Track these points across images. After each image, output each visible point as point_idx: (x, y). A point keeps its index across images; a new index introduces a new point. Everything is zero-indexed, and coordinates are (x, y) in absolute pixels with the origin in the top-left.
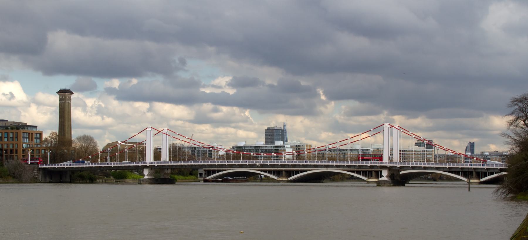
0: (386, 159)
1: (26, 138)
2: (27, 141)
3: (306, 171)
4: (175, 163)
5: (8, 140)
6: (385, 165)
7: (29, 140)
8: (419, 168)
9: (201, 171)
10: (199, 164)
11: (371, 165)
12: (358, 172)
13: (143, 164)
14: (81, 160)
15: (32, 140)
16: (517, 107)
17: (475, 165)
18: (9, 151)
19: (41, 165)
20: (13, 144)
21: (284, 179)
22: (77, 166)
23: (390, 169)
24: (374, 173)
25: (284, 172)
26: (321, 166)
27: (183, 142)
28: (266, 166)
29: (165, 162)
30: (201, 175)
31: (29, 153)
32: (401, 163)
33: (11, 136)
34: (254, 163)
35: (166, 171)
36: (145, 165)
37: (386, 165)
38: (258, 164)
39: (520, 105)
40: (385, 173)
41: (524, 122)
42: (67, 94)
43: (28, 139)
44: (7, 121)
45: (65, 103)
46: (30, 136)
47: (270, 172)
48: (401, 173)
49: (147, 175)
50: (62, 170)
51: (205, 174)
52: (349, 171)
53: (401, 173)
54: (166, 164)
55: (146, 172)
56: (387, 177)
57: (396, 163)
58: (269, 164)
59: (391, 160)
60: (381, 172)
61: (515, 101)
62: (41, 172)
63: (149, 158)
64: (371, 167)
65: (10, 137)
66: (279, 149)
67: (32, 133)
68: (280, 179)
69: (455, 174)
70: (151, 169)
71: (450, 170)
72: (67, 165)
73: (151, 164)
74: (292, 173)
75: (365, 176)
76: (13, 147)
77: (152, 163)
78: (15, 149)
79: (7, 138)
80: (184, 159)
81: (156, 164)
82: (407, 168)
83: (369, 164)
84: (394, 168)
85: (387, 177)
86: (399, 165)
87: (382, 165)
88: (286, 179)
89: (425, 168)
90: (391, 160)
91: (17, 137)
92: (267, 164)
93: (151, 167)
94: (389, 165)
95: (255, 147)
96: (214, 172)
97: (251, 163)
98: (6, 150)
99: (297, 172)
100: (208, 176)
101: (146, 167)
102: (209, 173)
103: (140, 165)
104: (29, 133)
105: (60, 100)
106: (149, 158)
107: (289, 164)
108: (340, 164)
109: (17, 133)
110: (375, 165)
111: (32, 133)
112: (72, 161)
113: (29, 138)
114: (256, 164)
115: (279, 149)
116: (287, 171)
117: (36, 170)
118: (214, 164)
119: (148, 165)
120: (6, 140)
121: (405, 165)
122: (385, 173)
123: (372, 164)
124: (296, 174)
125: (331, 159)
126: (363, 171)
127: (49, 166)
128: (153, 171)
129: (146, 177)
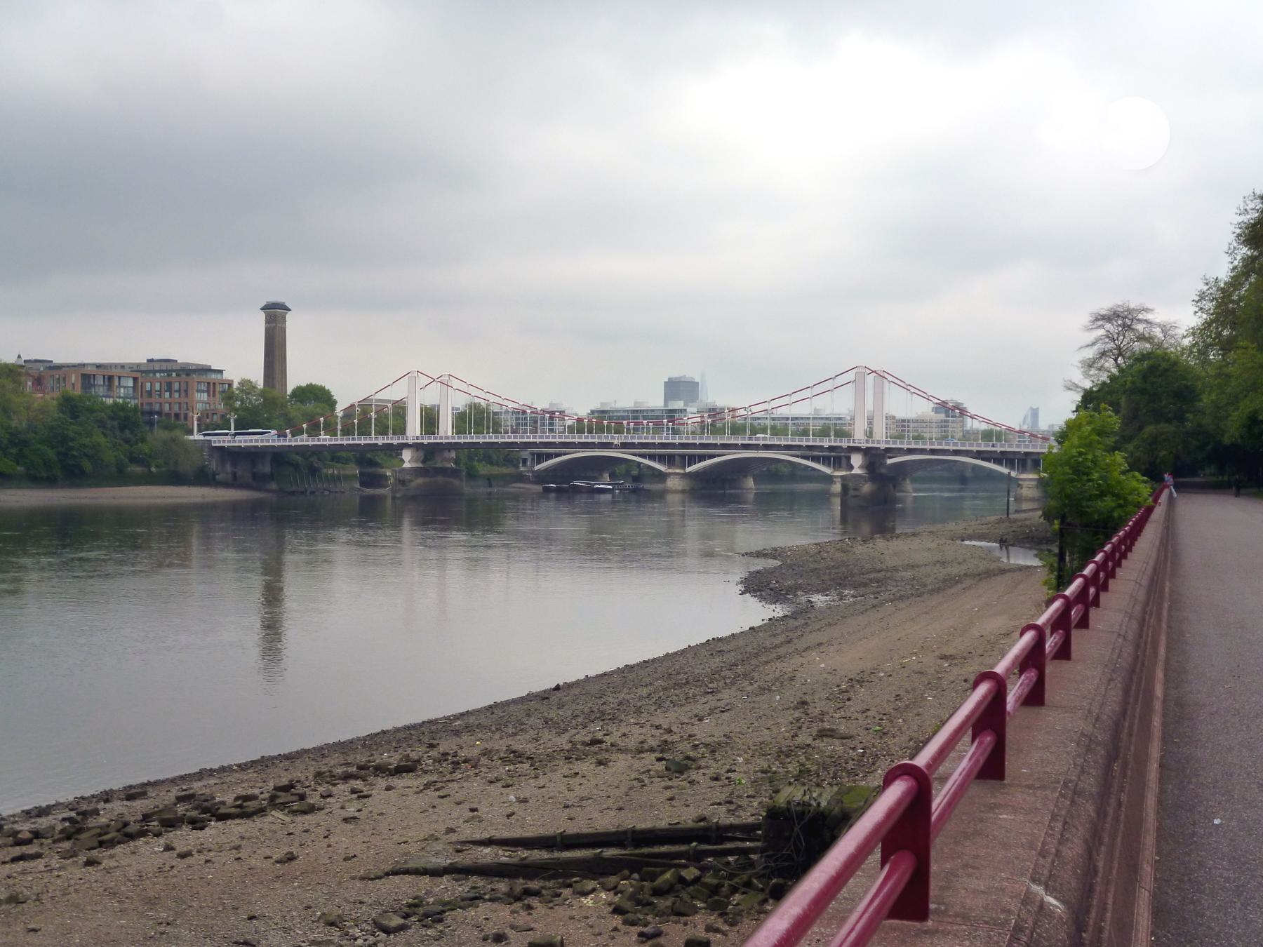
1: (204, 391)
2: (204, 396)
3: (719, 456)
4: (460, 438)
5: (171, 396)
7: (209, 395)
8: (922, 451)
9: (525, 454)
10: (506, 440)
11: (830, 444)
12: (816, 459)
13: (401, 441)
15: (214, 395)
16: (1101, 332)
17: (1027, 446)
18: (173, 415)
20: (180, 403)
21: (678, 471)
22: (280, 444)
23: (867, 452)
25: (677, 458)
26: (746, 447)
27: (477, 400)
28: (632, 446)
30: (525, 461)
31: (195, 419)
32: (887, 442)
34: (609, 441)
35: (446, 455)
36: (405, 441)
37: (859, 445)
38: (616, 442)
39: (1108, 326)
40: (857, 460)
41: (1116, 360)
43: (206, 394)
44: (176, 361)
45: (274, 327)
46: (211, 388)
47: (652, 457)
48: (889, 461)
50: (253, 450)
51: (533, 459)
52: (797, 456)
53: (889, 461)
55: (407, 455)
57: (878, 442)
58: (636, 441)
59: (869, 434)
60: (849, 458)
61: (1097, 320)
63: (414, 428)
64: (831, 448)
65: (176, 391)
66: (676, 415)
67: (214, 384)
68: (670, 471)
69: (994, 463)
70: (417, 450)
73: (416, 441)
74: (692, 459)
75: (829, 465)
76: (180, 409)
77: (418, 438)
78: (182, 413)
80: (496, 432)
81: (426, 441)
82: (900, 451)
83: (826, 444)
84: (874, 452)
85: (861, 467)
86: (883, 446)
87: (852, 445)
88: (682, 471)
89: (933, 452)
90: (869, 434)
91: (186, 391)
92: (633, 441)
93: (417, 447)
94: (864, 446)
95: (633, 411)
96: (549, 456)
97: (583, 440)
98: (168, 415)
99: (702, 458)
100: (539, 463)
101: (406, 446)
102: (540, 458)
103: (395, 441)
104: (209, 383)
105: (267, 322)
106: (414, 428)
107: (674, 441)
108: (709, 442)
109: (187, 382)
110: (838, 444)
111: (214, 384)
113: (208, 392)
114: (613, 441)
115: (676, 415)
116: (683, 456)
117: (206, 450)
118: (534, 440)
119: (410, 442)
120: (167, 395)
121: (894, 446)
122: (857, 460)
123: (833, 444)
124: (699, 462)
126: (824, 457)
128: (421, 454)
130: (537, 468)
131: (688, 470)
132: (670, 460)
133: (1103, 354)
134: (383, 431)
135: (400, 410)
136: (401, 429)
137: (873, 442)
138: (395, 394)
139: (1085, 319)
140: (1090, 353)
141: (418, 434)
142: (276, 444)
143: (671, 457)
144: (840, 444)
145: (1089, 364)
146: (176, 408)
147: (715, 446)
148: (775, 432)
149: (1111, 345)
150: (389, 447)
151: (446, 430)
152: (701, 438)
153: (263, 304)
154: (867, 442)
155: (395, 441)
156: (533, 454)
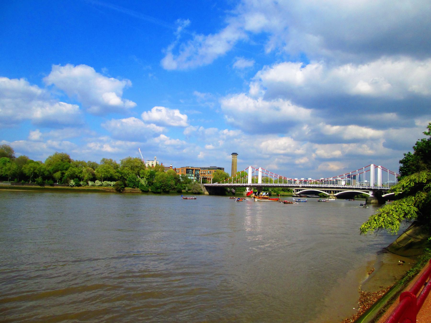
3: (343, 191)
6: (371, 188)
14: (221, 182)
19: (204, 184)
23: (374, 191)
25: (332, 192)
29: (260, 184)
30: (294, 191)
34: (298, 185)
36: (247, 185)
37: (371, 188)
38: (300, 186)
47: (325, 191)
49: (248, 190)
50: (213, 186)
51: (296, 191)
54: (261, 185)
55: (247, 188)
56: (372, 195)
62: (205, 187)
68: (330, 195)
72: (216, 184)
74: (336, 192)
85: (372, 195)
88: (333, 195)
90: (375, 185)
93: (249, 186)
94: (373, 188)
98: (208, 179)
100: (297, 191)
112: (217, 183)
116: (333, 191)
117: (202, 186)
130: (297, 193)
131: (335, 195)
132: (330, 192)
137: (377, 187)
141: (261, 183)
142: (217, 185)
143: (330, 191)
144: (365, 188)
146: (210, 177)
150: (243, 186)
151: (260, 183)
152: (330, 185)
154: (374, 187)
156: (296, 189)
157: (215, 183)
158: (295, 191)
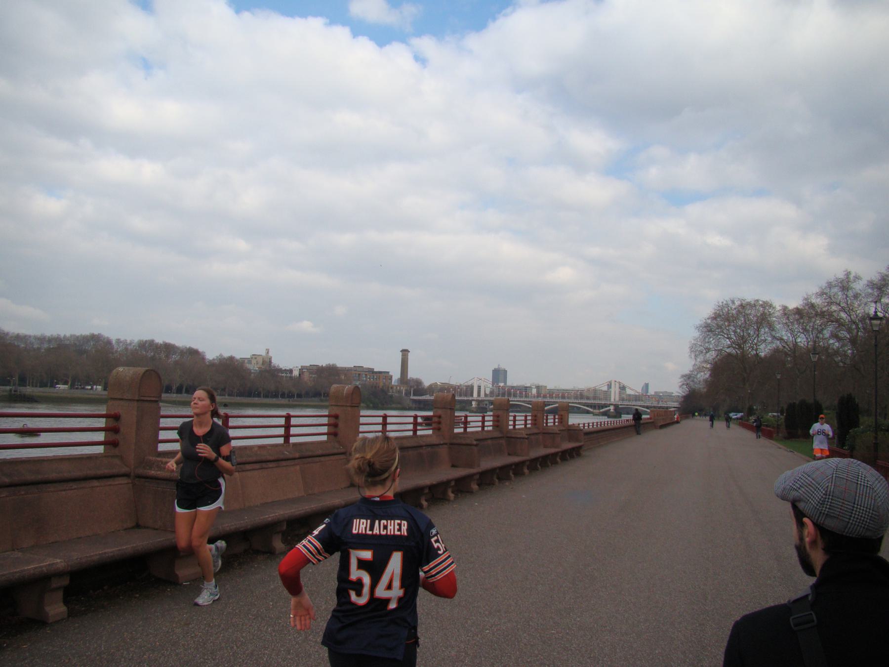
0: (612, 400)
8: (624, 405)
24: (597, 407)
33: (376, 377)
39: (685, 378)
42: (407, 352)
51: (489, 405)
55: (474, 403)
66: (528, 389)
71: (644, 407)
79: (373, 378)
89: (627, 405)
91: (379, 379)
93: (476, 400)
101: (474, 400)
105: (402, 355)
115: (528, 389)
125: (557, 396)
127: (412, 397)
128: (477, 403)
129: (473, 406)
133: (683, 384)
134: (466, 395)
135: (471, 388)
136: (472, 395)
138: (470, 383)
139: (679, 376)
140: (680, 384)
145: (680, 387)
147: (551, 402)
148: (576, 398)
149: (685, 383)
153: (401, 350)
155: (470, 398)
157: (424, 396)
158: (488, 403)
